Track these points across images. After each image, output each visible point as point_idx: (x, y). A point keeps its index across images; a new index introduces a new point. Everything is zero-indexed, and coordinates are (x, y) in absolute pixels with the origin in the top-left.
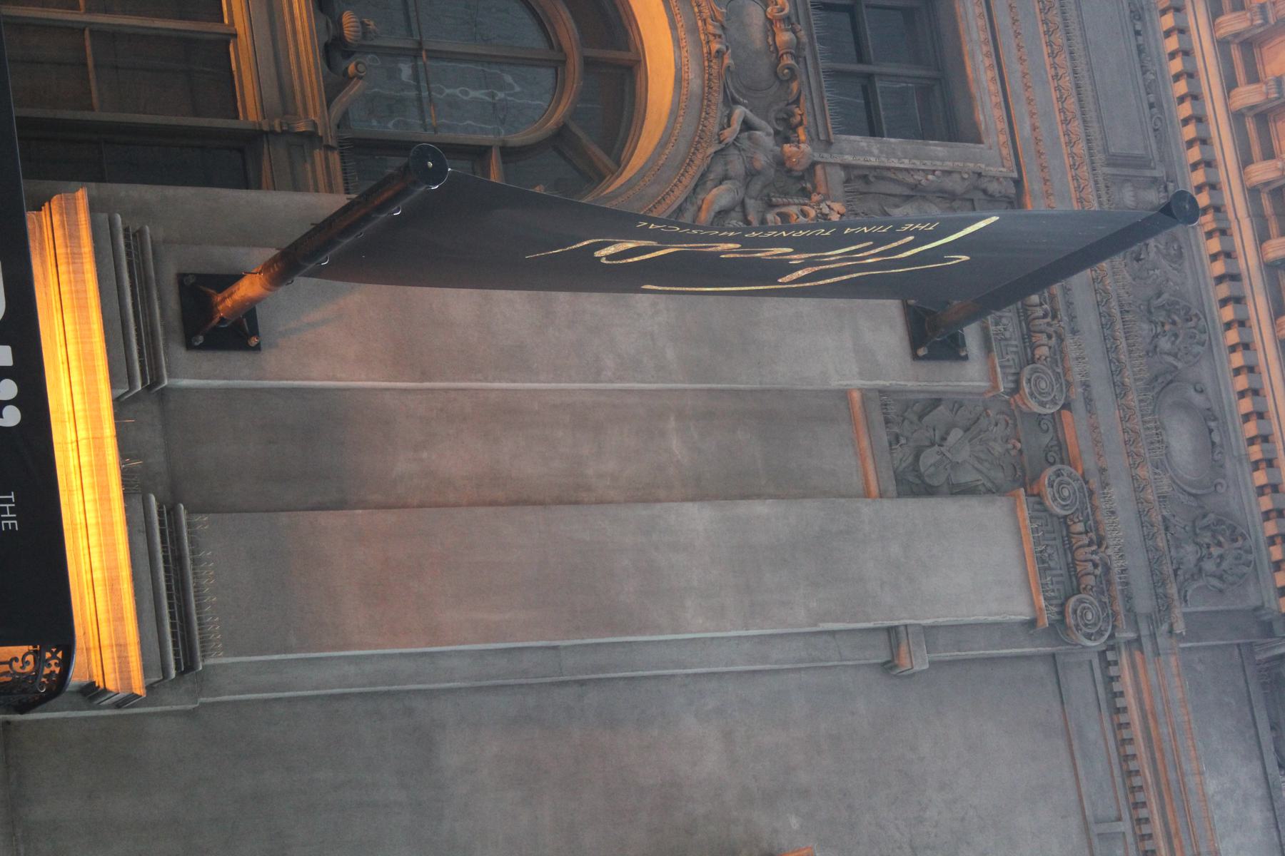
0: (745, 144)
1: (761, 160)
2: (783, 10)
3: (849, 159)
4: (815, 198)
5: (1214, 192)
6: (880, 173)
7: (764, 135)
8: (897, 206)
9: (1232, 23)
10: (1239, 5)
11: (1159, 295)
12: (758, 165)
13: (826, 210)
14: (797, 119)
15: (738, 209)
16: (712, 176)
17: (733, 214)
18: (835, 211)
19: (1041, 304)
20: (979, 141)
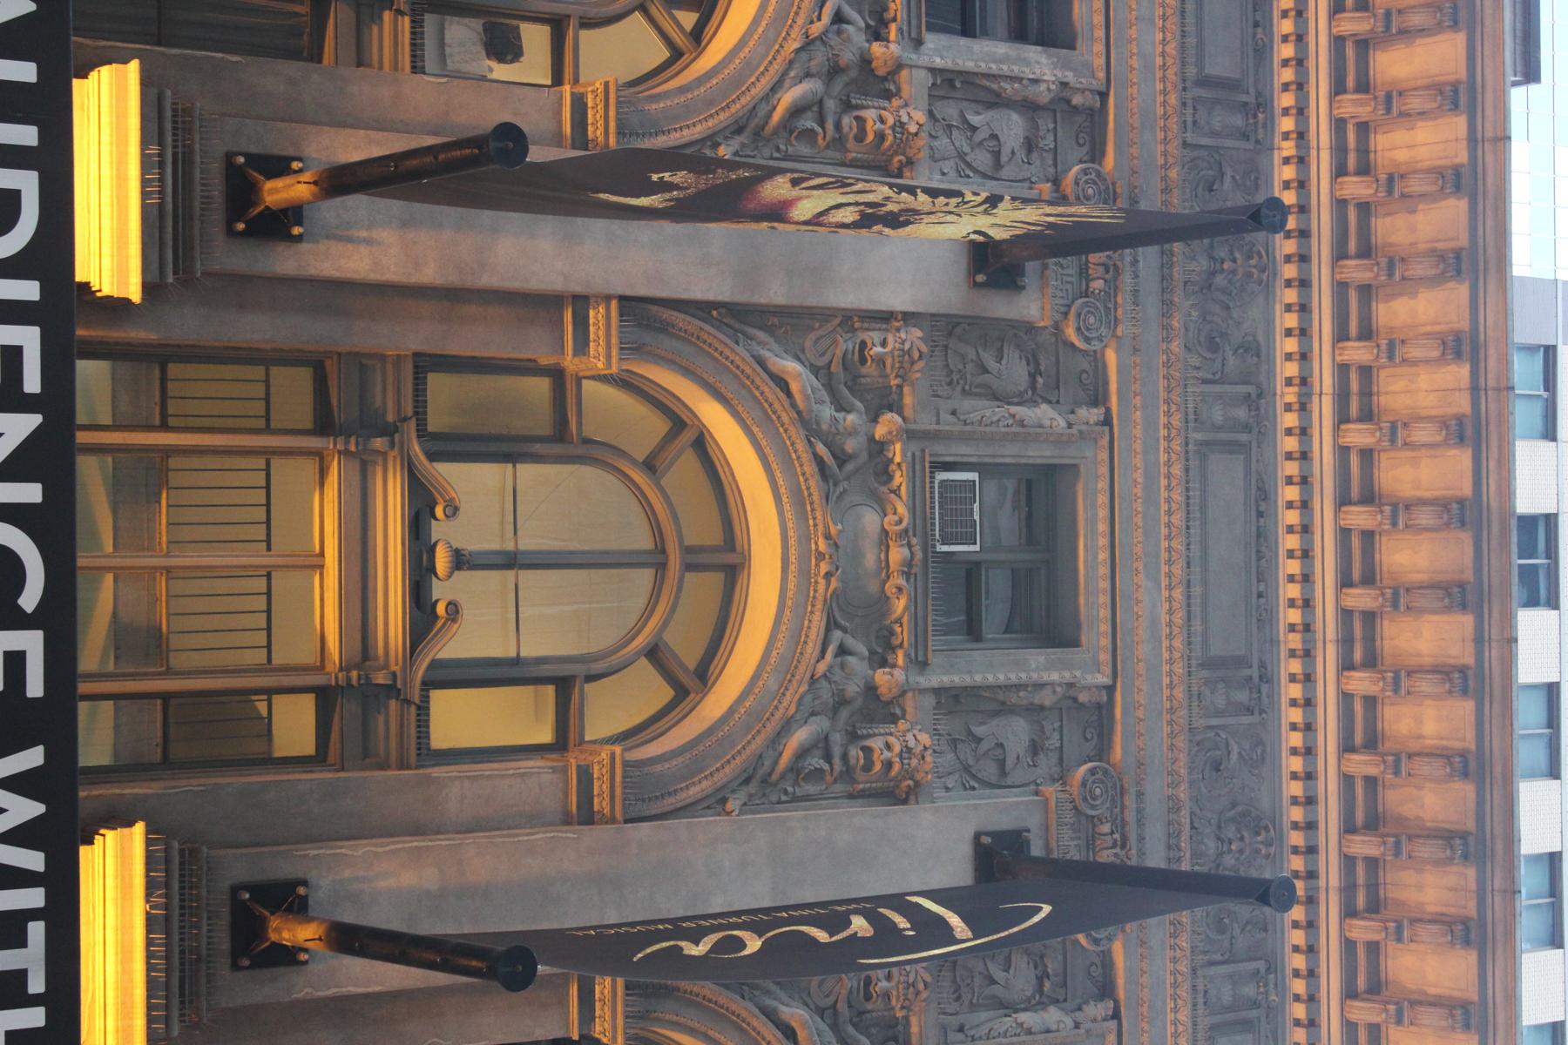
0: (834, 40)
1: (848, 56)
2: (900, 521)
3: (938, 62)
4: (896, 102)
5: (1304, 265)
6: (972, 691)
7: (855, 33)
8: (983, 723)
9: (1351, 24)
10: (1363, 5)
11: (1234, 805)
12: (842, 63)
13: (912, 743)
14: (890, 15)
15: (815, 109)
16: (792, 74)
17: (810, 114)
18: (916, 117)
19: (1112, 833)
20: (1072, 47)
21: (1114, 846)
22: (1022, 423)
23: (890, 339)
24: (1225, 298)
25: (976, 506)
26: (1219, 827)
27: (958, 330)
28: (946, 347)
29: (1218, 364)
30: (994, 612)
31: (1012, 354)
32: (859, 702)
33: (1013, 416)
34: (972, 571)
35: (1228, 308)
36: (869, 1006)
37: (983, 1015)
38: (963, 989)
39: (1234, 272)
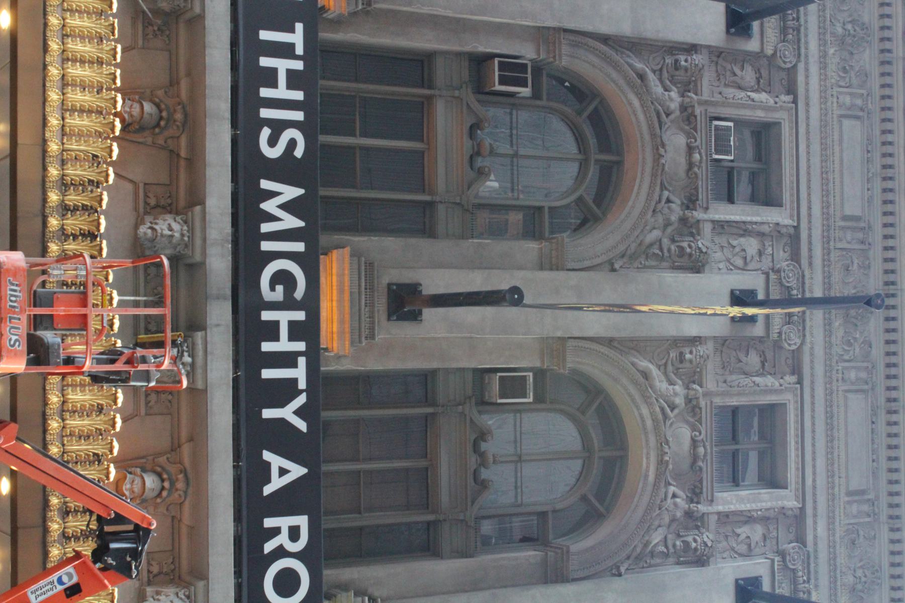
21: (793, 19)
22: (753, 100)
23: (689, 58)
24: (850, 48)
25: (732, 138)
26: (844, 24)
27: (723, 55)
28: (717, 63)
29: (847, 79)
30: (742, 188)
31: (749, 69)
32: (676, 225)
33: (749, 97)
34: (730, 172)
35: (852, 54)
36: (677, 73)
37: (731, 90)
38: (721, 77)
39: (854, 36)
